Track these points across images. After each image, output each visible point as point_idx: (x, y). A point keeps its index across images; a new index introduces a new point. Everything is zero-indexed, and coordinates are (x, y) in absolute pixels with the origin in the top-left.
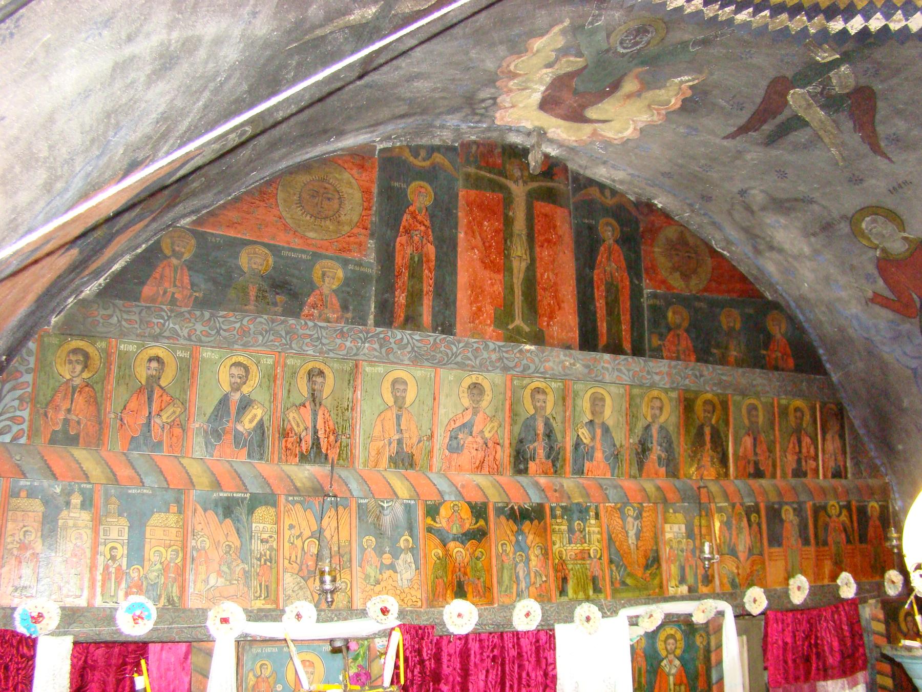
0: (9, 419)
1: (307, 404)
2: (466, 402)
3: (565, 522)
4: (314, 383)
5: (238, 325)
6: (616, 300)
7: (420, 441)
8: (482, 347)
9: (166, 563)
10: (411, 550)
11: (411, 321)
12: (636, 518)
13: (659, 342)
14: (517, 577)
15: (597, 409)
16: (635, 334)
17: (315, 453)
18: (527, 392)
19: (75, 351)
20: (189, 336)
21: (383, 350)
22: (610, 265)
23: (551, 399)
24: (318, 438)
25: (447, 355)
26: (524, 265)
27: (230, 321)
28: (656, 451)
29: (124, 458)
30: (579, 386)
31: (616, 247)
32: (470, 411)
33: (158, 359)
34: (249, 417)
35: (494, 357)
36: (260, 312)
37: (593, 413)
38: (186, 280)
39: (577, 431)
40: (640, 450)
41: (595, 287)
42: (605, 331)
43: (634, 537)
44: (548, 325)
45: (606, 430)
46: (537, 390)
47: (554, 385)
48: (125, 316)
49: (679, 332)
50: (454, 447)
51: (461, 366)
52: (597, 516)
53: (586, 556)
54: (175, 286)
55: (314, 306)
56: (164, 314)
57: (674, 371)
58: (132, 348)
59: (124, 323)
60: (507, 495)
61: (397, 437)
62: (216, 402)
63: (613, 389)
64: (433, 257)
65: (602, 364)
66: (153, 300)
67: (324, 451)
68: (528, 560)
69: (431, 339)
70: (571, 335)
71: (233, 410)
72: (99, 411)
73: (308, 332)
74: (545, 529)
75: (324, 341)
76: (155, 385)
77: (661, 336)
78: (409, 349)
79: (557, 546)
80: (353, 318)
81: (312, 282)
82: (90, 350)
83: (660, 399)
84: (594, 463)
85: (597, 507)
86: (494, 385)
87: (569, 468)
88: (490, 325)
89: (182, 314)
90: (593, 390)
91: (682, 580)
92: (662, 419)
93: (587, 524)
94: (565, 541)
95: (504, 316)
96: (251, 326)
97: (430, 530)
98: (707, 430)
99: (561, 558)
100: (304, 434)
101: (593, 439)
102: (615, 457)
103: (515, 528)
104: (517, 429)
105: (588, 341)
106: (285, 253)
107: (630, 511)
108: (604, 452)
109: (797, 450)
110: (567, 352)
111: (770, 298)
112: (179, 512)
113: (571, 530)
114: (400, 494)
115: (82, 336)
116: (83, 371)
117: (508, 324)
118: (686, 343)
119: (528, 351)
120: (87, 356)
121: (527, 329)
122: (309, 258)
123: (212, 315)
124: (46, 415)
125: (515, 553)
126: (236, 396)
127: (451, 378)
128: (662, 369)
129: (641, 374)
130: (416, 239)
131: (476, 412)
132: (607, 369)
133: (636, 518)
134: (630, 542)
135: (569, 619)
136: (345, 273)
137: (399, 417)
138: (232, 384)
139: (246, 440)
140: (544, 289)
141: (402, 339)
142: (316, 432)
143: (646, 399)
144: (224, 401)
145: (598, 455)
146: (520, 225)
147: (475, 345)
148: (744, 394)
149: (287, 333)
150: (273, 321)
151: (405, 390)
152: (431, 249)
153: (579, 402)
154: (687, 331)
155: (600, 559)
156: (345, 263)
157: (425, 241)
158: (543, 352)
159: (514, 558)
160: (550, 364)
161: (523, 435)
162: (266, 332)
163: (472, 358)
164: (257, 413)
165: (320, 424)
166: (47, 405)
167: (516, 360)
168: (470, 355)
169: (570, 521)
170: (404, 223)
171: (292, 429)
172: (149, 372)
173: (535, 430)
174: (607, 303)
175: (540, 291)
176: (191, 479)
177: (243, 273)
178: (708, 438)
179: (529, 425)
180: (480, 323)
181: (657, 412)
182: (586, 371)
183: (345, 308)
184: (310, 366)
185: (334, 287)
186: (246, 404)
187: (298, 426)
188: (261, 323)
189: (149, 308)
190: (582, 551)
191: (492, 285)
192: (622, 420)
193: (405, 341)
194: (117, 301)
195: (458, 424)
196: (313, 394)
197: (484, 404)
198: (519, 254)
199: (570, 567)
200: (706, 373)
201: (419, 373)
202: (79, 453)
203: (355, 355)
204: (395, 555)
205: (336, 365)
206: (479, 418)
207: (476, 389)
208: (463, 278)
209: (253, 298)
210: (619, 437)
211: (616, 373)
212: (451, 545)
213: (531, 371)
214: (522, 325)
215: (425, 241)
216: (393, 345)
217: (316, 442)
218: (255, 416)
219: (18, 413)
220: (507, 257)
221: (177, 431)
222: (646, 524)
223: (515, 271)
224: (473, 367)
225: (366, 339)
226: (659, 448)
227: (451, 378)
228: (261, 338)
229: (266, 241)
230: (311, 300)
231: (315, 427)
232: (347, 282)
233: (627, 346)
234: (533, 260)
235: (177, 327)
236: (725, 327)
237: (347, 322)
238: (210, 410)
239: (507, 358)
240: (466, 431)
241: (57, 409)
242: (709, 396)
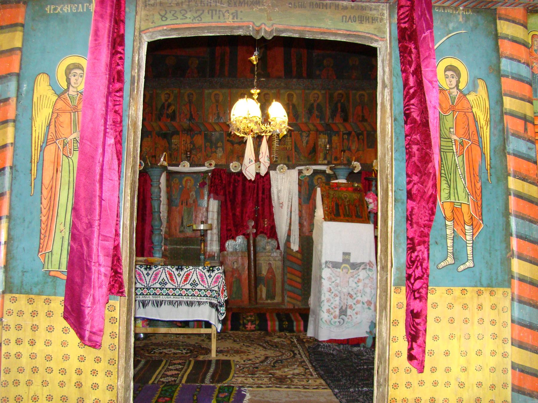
10: (222, 147)
12: (307, 137)
71: (166, 108)
91: (325, 158)
92: (318, 102)
97: (228, 141)
98: (339, 105)
107: (304, 134)
112: (151, 137)
114: (217, 129)
126: (167, 103)
133: (307, 137)
135: (275, 170)
142: (191, 112)
144: (163, 105)
164: (173, 107)
165: (192, 110)
184: (188, 92)
186: (169, 105)
190: (284, 148)
204: (217, 148)
212: (235, 145)
238: (159, 107)
242: (340, 92)
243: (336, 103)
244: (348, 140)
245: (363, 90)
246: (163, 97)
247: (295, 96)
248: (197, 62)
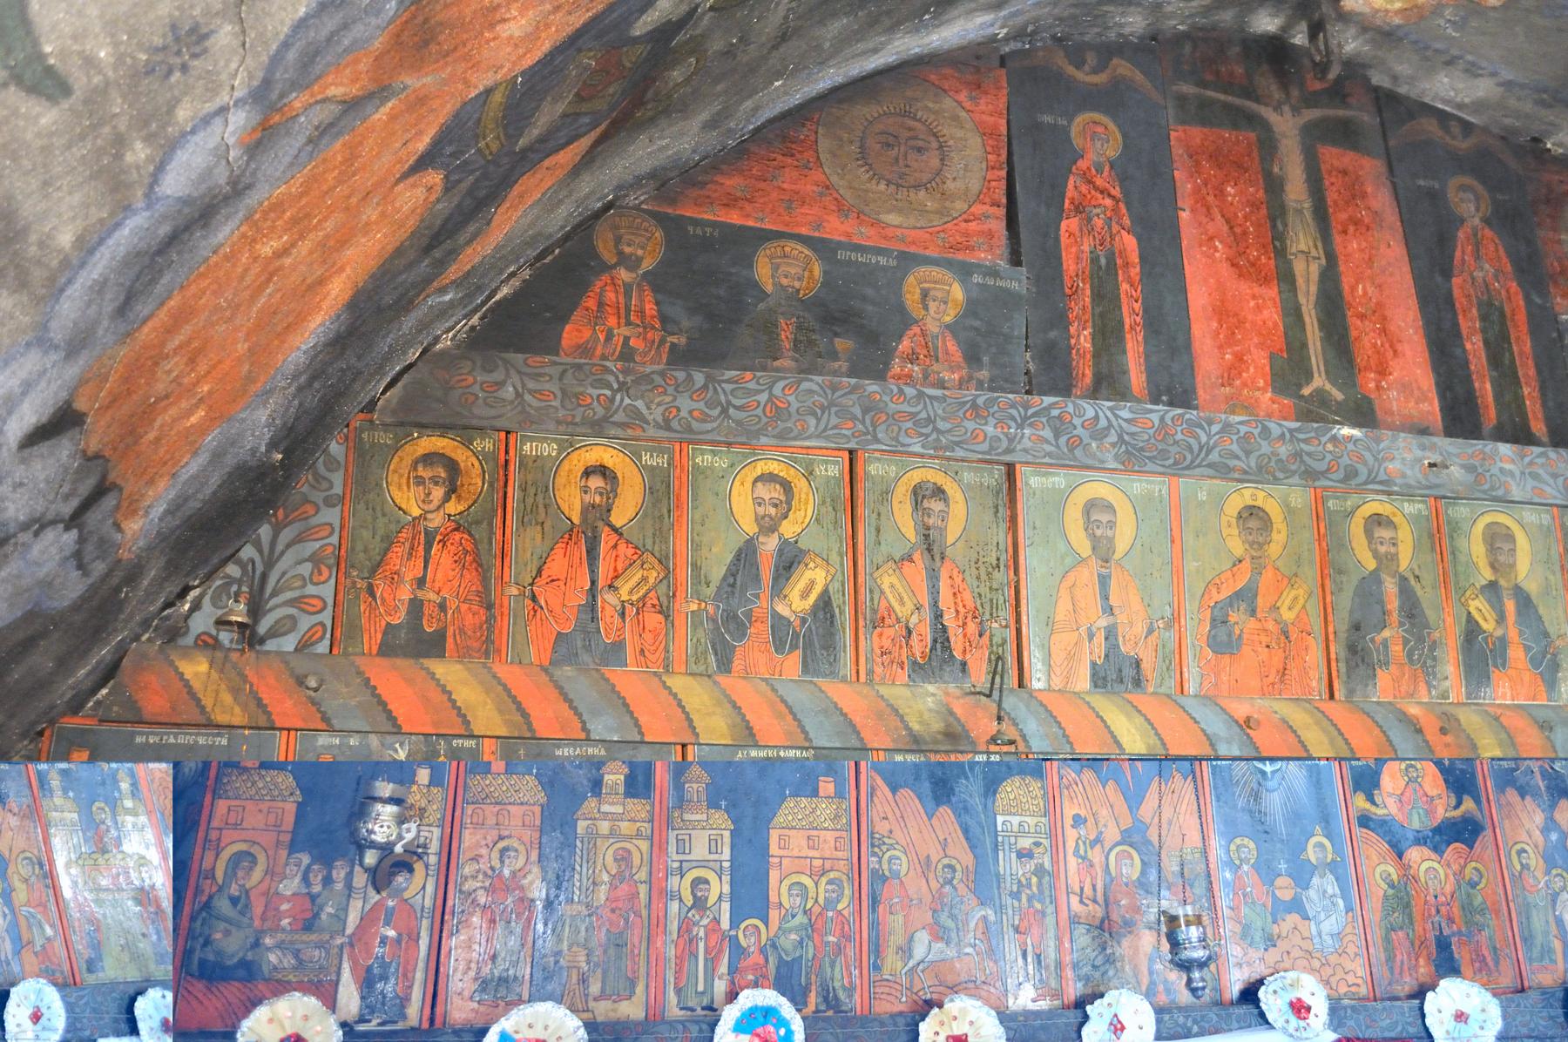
0: (291, 603)
1: (917, 556)
2: (1237, 547)
4: (927, 512)
5: (763, 397)
6: (1504, 337)
7: (1150, 631)
8: (1256, 432)
9: (817, 910)
11: (1108, 384)
15: (1502, 558)
17: (939, 657)
18: (1357, 527)
19: (429, 459)
20: (667, 421)
21: (1063, 440)
22: (1482, 267)
23: (1405, 535)
24: (944, 629)
25: (1190, 448)
26: (1315, 269)
27: (749, 390)
29: (544, 678)
30: (1461, 511)
31: (1488, 232)
32: (1247, 564)
33: (602, 471)
34: (801, 585)
35: (1284, 450)
36: (808, 370)
37: (1493, 566)
38: (650, 308)
39: (1465, 605)
41: (1459, 311)
44: (1378, 387)
45: (1525, 602)
46: (1377, 520)
47: (1409, 508)
48: (531, 385)
50: (1223, 642)
51: (1222, 471)
54: (628, 323)
55: (912, 358)
56: (611, 378)
58: (549, 449)
59: (527, 397)
60: (1347, 743)
61: (1103, 622)
62: (729, 557)
63: (1530, 516)
64: (1135, 258)
66: (584, 350)
67: (957, 655)
69: (1155, 418)
70: (1425, 407)
71: (767, 574)
72: (485, 580)
73: (905, 408)
75: (941, 425)
76: (600, 524)
78: (1113, 438)
80: (992, 380)
81: (901, 310)
82: (461, 456)
86: (1289, 511)
88: (1264, 390)
89: (647, 378)
90: (1488, 519)
95: (1289, 371)
96: (791, 399)
100: (914, 620)
101: (1501, 619)
105: (1460, 418)
106: (842, 255)
108: (1527, 649)
110: (1426, 440)
115: (444, 429)
116: (447, 499)
117: (1300, 387)
119: (1350, 438)
120: (452, 467)
121: (1339, 396)
122: (893, 263)
123: (709, 378)
124: (371, 591)
126: (770, 544)
127: (1202, 496)
130: (1098, 223)
132: (1511, 474)
136: (967, 291)
137: (1104, 581)
138: (758, 519)
139: (796, 635)
140: (1362, 317)
141: (1097, 417)
142: (938, 616)
144: (746, 556)
145: (1516, 654)
146: (1296, 191)
147: (1243, 429)
149: (865, 411)
150: (834, 389)
151: (1112, 525)
152: (1129, 242)
153: (1462, 543)
156: (964, 271)
157: (1115, 228)
158: (1378, 441)
162: (823, 409)
163: (1241, 454)
164: (814, 577)
165: (946, 600)
166: (373, 571)
168: (1235, 447)
170: (1070, 192)
171: (890, 609)
172: (587, 498)
173: (1381, 602)
174: (1486, 343)
175: (1353, 321)
176: (690, 721)
177: (763, 295)
179: (1369, 588)
180: (1245, 385)
182: (1471, 478)
183: (972, 357)
184: (916, 476)
185: (948, 319)
186: (790, 561)
187: (902, 603)
188: (811, 391)
189: (579, 367)
191: (1259, 308)
193: (1103, 423)
194: (511, 356)
195: (1225, 594)
196: (927, 536)
197: (1274, 549)
198: (1303, 247)
201: (1138, 486)
202: (447, 670)
203: (1008, 451)
205: (967, 476)
206: (1268, 574)
208: (1199, 298)
209: (787, 345)
211: (1531, 483)
214: (1328, 387)
215: (1115, 228)
216: (1080, 431)
217: (941, 638)
218: (812, 583)
219: (311, 589)
220: (1281, 253)
221: (653, 620)
223: (1300, 282)
224: (1245, 472)
225: (1026, 418)
227: (1202, 496)
228: (812, 422)
229: (804, 231)
230: (905, 345)
231: (935, 604)
232: (972, 308)
233: (1539, 428)
234: (1331, 257)
235: (639, 404)
237: (980, 385)
238: (717, 572)
239: (1309, 454)
241: (395, 579)
246: (743, 504)
247: (1522, 541)
248: (958, 292)
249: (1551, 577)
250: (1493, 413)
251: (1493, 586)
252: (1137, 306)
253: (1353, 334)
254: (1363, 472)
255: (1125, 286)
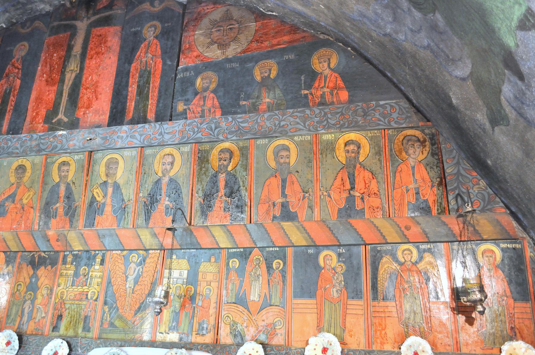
2: (13, 179)
3: (73, 267)
12: (140, 264)
13: (185, 107)
14: (23, 311)
15: (111, 172)
16: (161, 105)
23: (73, 168)
26: (74, 75)
28: (165, 202)
31: (155, 41)
37: (107, 175)
40: (148, 203)
42: (132, 108)
43: (132, 282)
45: (117, 187)
46: (64, 163)
49: (205, 94)
52: (102, 262)
53: (84, 297)
57: (187, 128)
60: (23, 246)
65: (119, 134)
68: (35, 298)
74: (55, 274)
77: (187, 101)
79: (61, 288)
83: (172, 155)
84: (104, 216)
85: (103, 256)
86: (33, 164)
87: (81, 222)
88: (41, 123)
90: (109, 157)
92: (172, 174)
93: (92, 269)
94: (69, 283)
98: (222, 177)
99: (62, 298)
101: (105, 196)
102: (122, 210)
103: (31, 272)
104: (45, 194)
108: (113, 206)
109: (348, 186)
111: (48, 8)
113: (76, 274)
118: (212, 101)
121: (66, 120)
125: (26, 293)
128: (177, 128)
129: (152, 136)
131: (19, 185)
133: (140, 264)
134: (127, 286)
143: (158, 156)
145: (108, 209)
147: (24, 139)
148: (269, 135)
152: (18, 82)
153: (96, 168)
154: (215, 91)
155: (96, 300)
159: (24, 297)
160: (75, 142)
161: (49, 200)
163: (19, 148)
167: (49, 143)
169: (77, 267)
170: (7, 71)
173: (58, 194)
174: (138, 86)
178: (222, 184)
180: (36, 123)
181: (168, 167)
190: (81, 293)
192: (133, 177)
195: (6, 196)
197: (25, 179)
198: (72, 68)
199: (67, 306)
200: (223, 125)
206: (21, 188)
207: (21, 168)
210: (128, 193)
211: (129, 139)
213: (57, 149)
215: (16, 78)
222: (147, 269)
223: (66, 81)
224: (18, 153)
226: (167, 198)
234: (82, 69)
236: (258, 78)
239: (42, 144)
240: (11, 200)
242: (226, 145)
243: (215, 176)
244: (241, 272)
245: (284, 134)
247: (121, 164)
249: (131, 177)
250: (131, 114)
251: (105, 182)
252: (13, 103)
253: (81, 95)
254: (59, 146)
255: (12, 97)
